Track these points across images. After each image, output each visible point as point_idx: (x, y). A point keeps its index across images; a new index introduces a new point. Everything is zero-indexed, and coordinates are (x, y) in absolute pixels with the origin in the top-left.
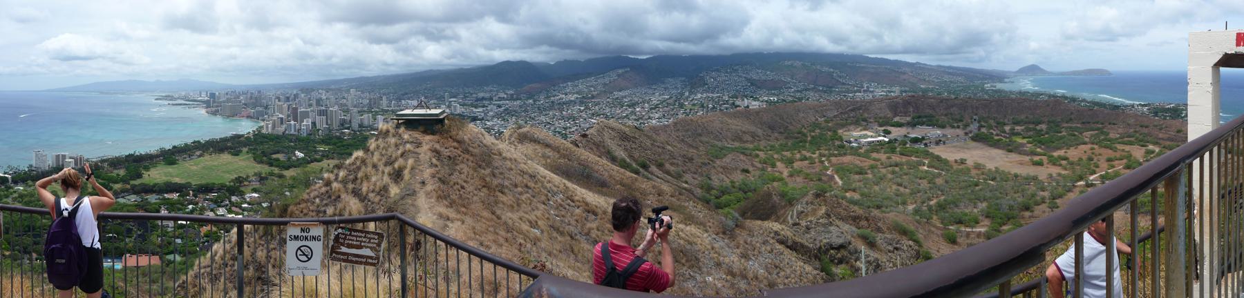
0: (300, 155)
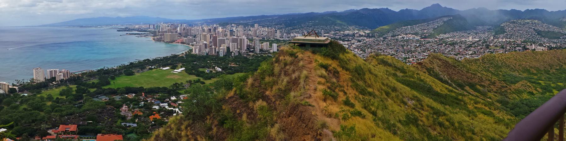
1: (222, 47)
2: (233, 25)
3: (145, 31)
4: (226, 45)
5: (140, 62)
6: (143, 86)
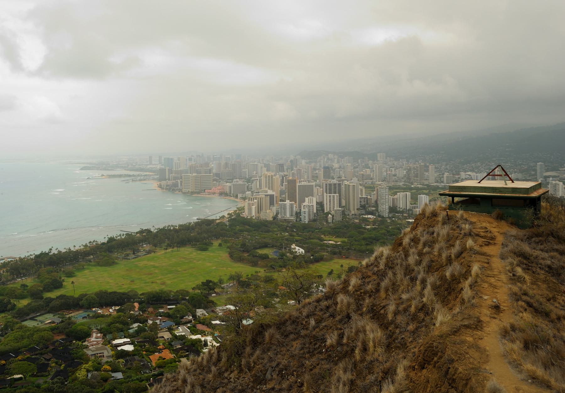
1: (306, 203)
2: (331, 156)
6: (134, 287)
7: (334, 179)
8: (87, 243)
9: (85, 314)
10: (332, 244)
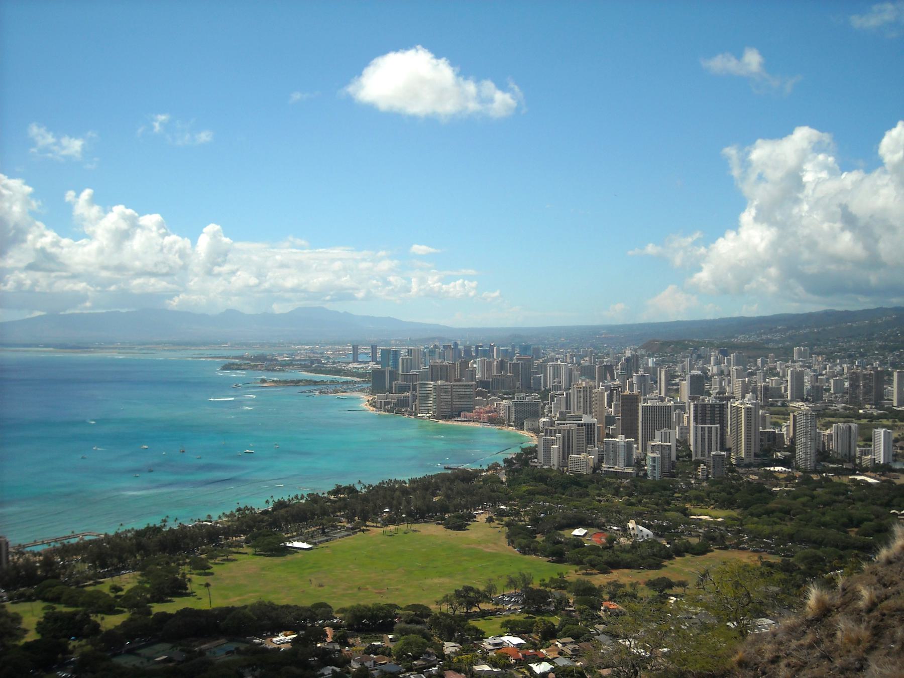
0: (639, 530)
3: (338, 372)
4: (676, 433)
5: (314, 499)
7: (710, 395)
8: (234, 511)
9: (232, 646)
10: (706, 521)
